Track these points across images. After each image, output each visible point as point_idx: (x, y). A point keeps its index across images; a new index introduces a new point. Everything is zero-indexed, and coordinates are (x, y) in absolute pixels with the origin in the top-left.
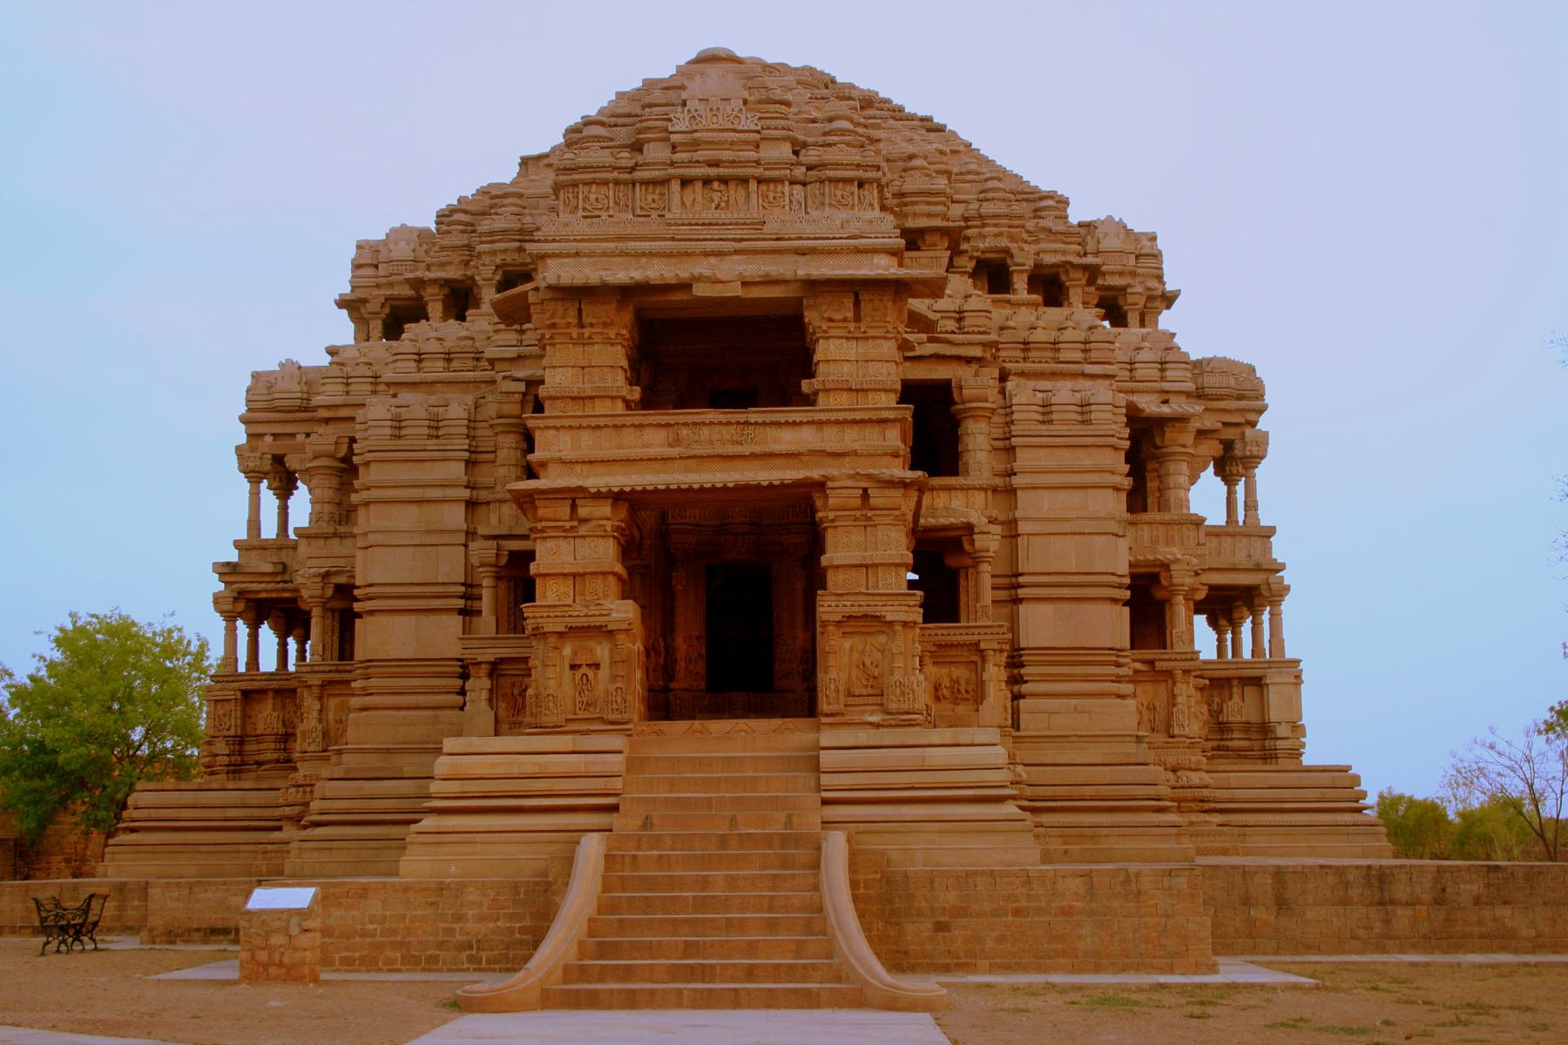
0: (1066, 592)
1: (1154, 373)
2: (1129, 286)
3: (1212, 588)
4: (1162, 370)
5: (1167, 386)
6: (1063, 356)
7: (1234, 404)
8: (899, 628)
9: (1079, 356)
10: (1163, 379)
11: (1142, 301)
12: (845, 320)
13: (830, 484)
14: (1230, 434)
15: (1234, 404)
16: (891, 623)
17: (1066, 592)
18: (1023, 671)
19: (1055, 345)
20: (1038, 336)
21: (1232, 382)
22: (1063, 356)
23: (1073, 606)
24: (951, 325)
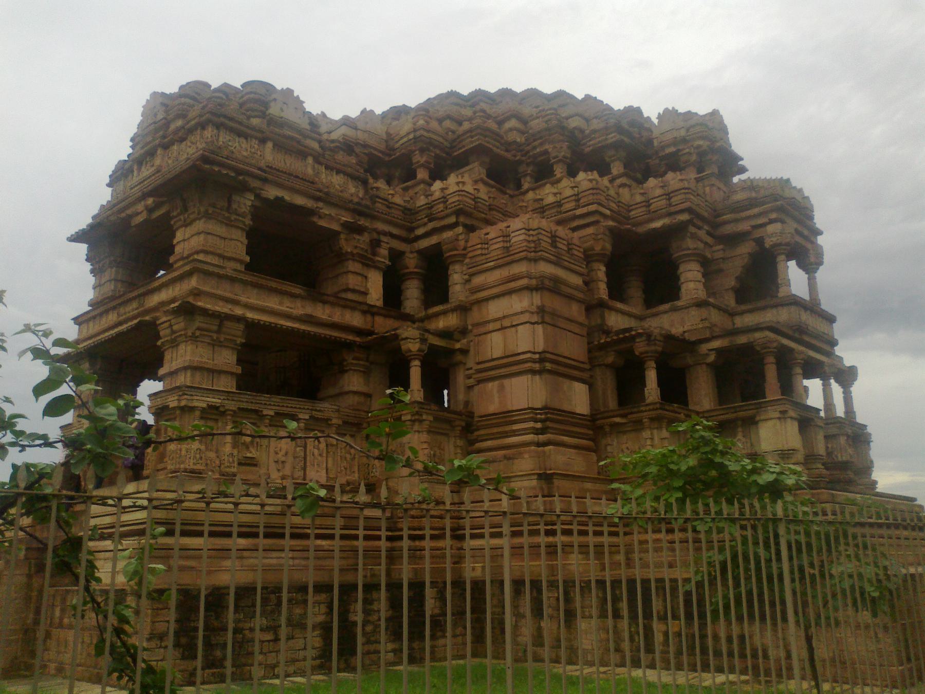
0: (503, 371)
1: (663, 203)
2: (679, 150)
3: (719, 351)
4: (669, 199)
5: (673, 209)
6: (564, 208)
7: (755, 211)
8: (178, 412)
9: (572, 205)
10: (670, 205)
11: (694, 158)
12: (179, 214)
13: (158, 322)
14: (757, 234)
15: (755, 211)
16: (174, 408)
17: (503, 371)
18: (476, 433)
19: (559, 204)
20: (551, 199)
21: (754, 195)
22: (564, 208)
23: (506, 382)
24: (441, 206)
